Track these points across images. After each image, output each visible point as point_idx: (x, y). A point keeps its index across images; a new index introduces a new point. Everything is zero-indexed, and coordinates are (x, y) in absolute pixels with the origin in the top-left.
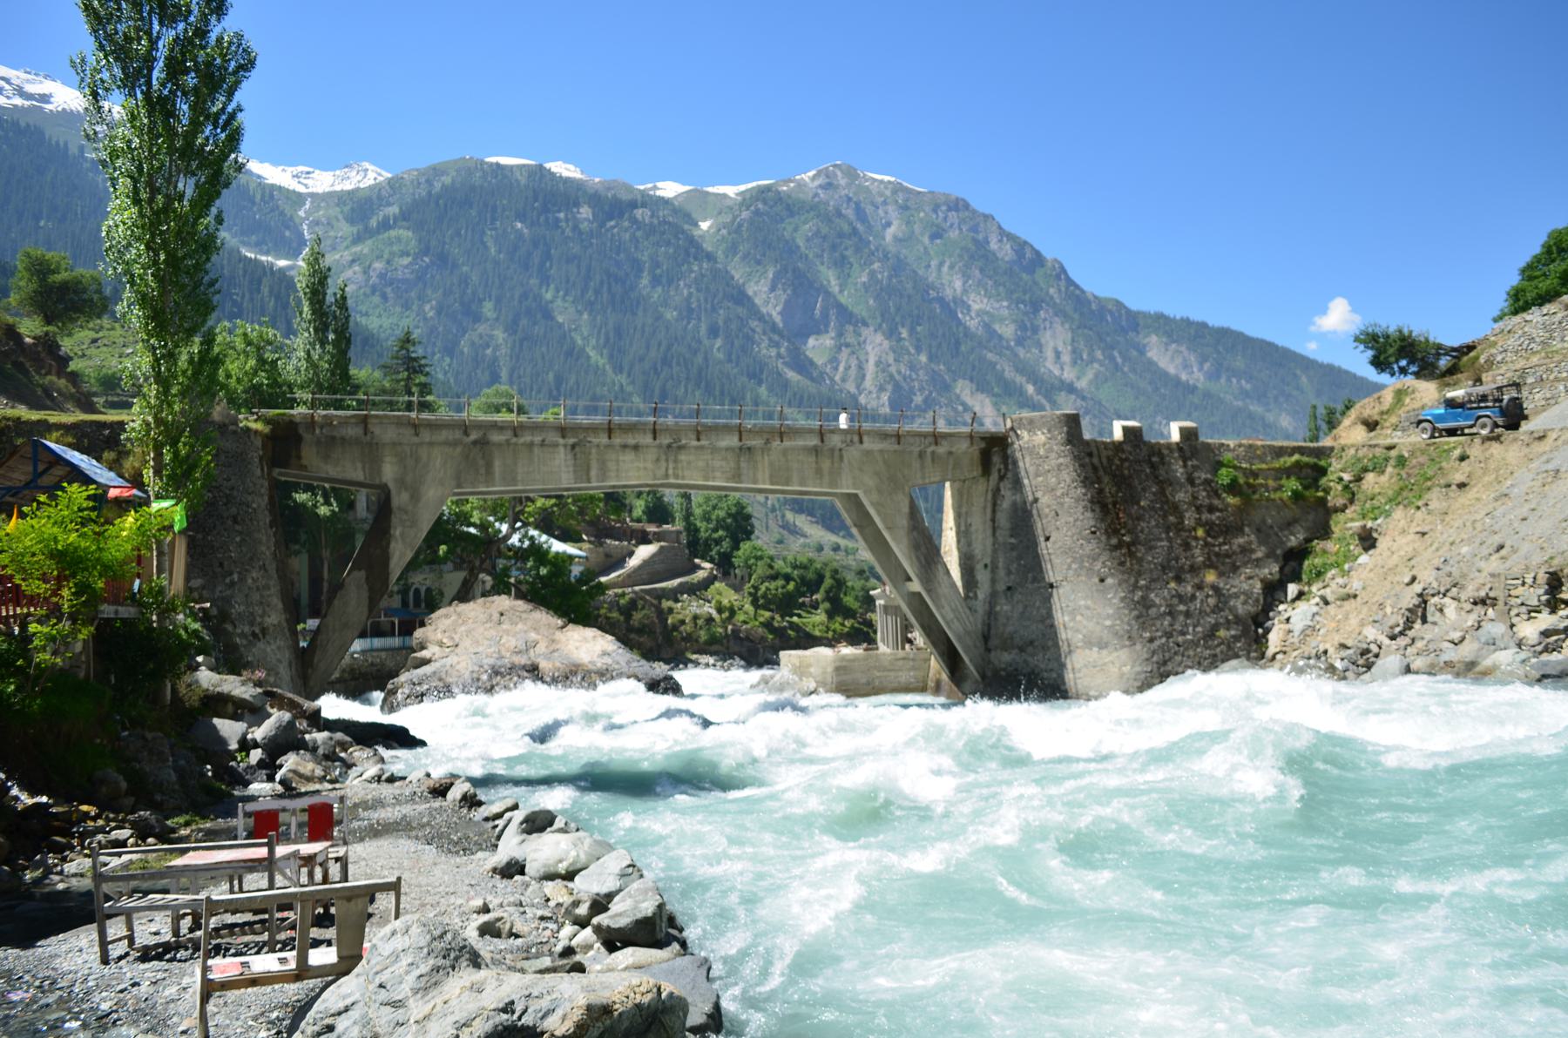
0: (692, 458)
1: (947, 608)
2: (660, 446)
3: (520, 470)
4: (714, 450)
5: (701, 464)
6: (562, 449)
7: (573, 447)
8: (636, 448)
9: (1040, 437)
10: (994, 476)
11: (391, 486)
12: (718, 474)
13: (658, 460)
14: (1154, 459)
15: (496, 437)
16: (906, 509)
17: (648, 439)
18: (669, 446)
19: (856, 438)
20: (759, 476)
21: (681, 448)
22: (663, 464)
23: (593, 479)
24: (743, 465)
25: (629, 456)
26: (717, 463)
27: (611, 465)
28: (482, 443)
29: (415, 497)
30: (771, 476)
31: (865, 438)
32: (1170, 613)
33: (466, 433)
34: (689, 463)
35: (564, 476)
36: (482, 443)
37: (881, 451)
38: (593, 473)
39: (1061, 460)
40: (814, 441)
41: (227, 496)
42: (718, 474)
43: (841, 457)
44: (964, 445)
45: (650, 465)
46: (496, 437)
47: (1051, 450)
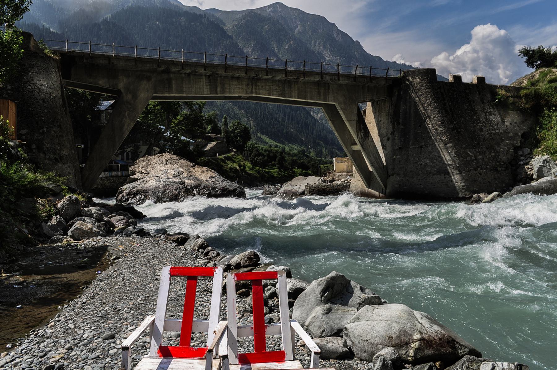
0: (263, 84)
1: (372, 157)
2: (249, 78)
3: (184, 87)
4: (273, 81)
5: (267, 87)
6: (204, 77)
7: (209, 76)
8: (238, 78)
9: (417, 80)
10: (394, 98)
11: (122, 90)
12: (275, 92)
13: (248, 85)
14: (467, 91)
15: (174, 69)
16: (356, 112)
17: (243, 75)
18: (253, 78)
19: (337, 78)
20: (293, 95)
21: (259, 79)
22: (251, 87)
23: (219, 92)
24: (286, 89)
25: (235, 82)
26: (275, 88)
27: (227, 86)
28: (167, 71)
29: (135, 97)
30: (298, 94)
31: (341, 78)
32: (476, 160)
33: (159, 66)
34: (262, 87)
35: (205, 90)
36: (167, 71)
37: (346, 85)
38: (219, 89)
39: (427, 90)
40: (317, 79)
41: (39, 89)
42: (275, 92)
43: (329, 87)
44: (383, 83)
45: (244, 87)
46: (174, 69)
47: (422, 85)
